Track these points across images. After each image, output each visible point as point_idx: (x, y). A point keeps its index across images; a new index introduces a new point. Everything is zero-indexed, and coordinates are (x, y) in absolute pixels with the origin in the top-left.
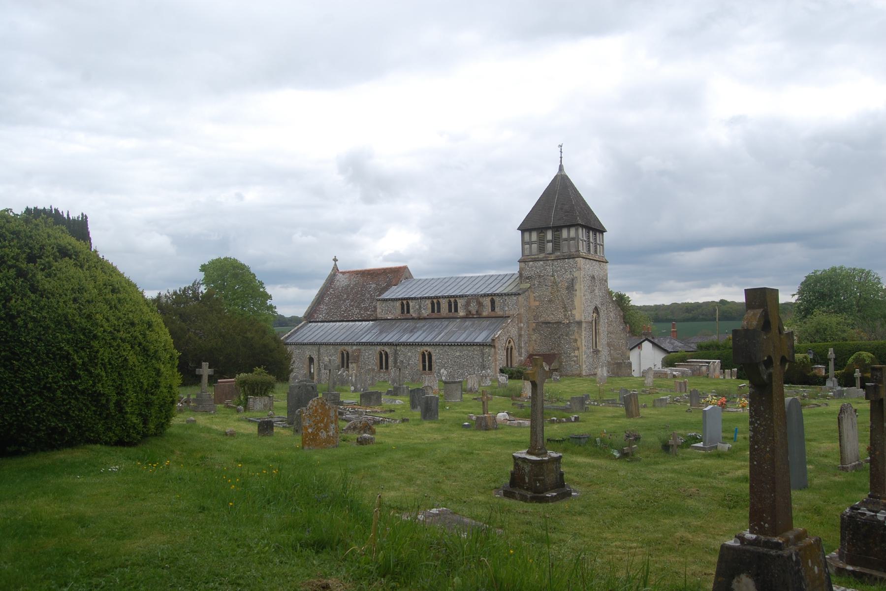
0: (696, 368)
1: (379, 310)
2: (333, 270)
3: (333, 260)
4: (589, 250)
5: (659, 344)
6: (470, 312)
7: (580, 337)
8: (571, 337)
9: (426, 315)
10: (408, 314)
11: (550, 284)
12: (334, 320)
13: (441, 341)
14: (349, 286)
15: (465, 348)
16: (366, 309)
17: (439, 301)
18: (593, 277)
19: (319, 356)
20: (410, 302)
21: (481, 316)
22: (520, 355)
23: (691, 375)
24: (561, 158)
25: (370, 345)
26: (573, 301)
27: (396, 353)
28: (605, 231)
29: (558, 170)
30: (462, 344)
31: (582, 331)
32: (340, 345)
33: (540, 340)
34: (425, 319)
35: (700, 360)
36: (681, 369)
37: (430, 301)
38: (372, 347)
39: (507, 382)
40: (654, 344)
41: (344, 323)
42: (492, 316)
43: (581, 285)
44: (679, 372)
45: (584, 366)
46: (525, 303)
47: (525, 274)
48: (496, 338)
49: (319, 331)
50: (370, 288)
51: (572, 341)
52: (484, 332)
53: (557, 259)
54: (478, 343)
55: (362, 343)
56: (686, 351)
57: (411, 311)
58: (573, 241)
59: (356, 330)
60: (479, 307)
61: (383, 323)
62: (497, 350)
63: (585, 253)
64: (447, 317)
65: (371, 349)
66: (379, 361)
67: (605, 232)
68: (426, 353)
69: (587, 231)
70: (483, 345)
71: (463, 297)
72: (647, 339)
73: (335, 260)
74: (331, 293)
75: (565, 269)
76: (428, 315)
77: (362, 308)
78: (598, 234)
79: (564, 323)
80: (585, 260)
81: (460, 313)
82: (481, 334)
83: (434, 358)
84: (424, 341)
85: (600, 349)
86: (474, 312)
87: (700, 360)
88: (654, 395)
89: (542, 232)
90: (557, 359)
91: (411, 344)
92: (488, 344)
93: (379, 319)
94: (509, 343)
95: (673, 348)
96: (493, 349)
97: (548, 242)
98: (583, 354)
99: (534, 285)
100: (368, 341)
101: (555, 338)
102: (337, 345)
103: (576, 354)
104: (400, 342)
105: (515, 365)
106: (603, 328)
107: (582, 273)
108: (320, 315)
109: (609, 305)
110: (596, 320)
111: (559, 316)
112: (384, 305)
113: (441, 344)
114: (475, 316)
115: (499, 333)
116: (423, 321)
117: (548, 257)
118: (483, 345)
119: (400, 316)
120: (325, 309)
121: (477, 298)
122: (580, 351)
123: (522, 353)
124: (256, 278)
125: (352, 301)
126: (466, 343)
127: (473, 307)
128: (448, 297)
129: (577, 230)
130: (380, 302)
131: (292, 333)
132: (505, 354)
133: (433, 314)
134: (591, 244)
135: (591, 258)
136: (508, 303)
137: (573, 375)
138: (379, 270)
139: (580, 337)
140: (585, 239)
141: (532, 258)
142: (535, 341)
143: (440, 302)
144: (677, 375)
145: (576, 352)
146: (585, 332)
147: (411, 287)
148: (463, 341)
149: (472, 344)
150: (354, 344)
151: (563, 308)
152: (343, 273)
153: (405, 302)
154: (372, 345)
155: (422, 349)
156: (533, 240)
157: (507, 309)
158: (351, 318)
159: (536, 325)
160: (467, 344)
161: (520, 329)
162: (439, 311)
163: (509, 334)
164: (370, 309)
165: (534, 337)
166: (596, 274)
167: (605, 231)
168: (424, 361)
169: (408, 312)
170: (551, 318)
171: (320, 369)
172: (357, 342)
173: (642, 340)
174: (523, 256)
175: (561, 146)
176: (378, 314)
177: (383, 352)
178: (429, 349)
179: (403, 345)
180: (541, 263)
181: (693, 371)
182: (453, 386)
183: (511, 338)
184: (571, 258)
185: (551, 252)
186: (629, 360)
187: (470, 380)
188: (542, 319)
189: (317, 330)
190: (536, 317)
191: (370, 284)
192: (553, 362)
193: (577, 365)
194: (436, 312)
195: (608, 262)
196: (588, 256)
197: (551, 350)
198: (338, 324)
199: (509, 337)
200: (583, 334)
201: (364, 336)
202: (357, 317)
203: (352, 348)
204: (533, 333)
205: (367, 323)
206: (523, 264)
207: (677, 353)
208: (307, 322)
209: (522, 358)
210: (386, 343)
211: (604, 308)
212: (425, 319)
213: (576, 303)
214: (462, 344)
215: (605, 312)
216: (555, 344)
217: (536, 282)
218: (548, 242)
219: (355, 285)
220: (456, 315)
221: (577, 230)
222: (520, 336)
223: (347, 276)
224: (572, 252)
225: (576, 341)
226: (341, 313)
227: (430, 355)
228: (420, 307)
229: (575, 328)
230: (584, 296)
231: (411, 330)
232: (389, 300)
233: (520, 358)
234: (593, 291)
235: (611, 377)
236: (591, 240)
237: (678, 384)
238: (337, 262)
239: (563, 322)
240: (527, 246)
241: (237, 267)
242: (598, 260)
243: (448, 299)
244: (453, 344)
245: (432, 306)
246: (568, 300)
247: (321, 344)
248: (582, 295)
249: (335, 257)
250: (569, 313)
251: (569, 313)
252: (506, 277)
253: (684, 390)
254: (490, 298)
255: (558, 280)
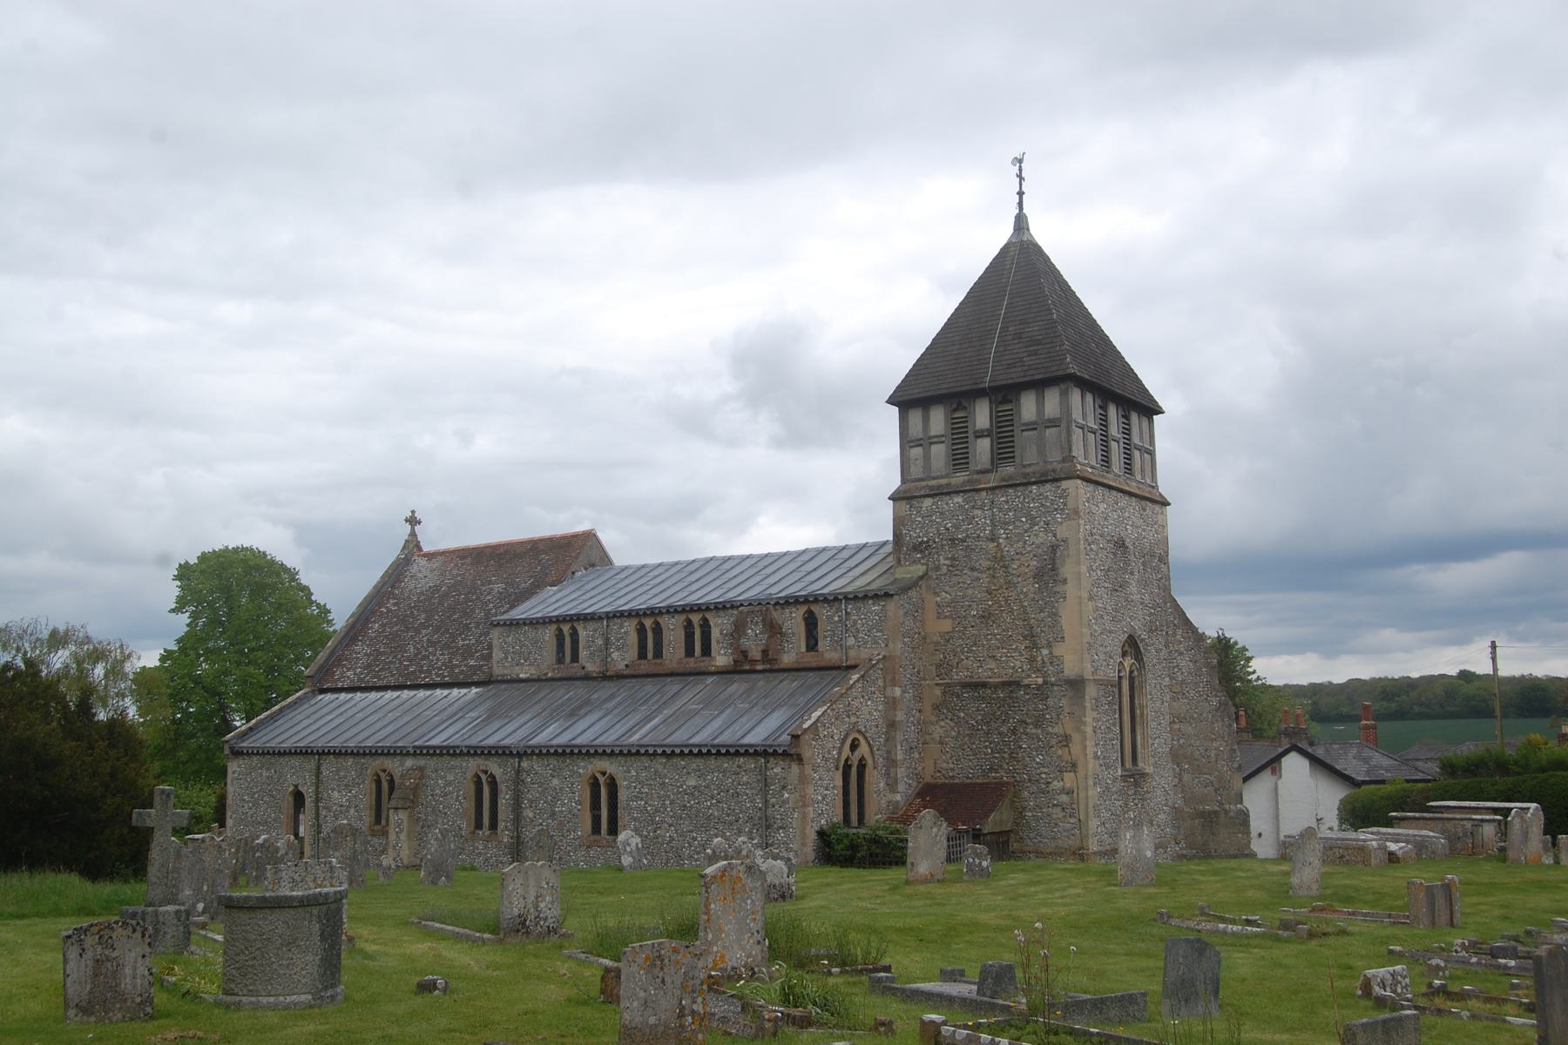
0: (1460, 830)
1: (497, 654)
2: (404, 547)
3: (407, 520)
4: (1106, 461)
5: (1328, 761)
6: (744, 653)
7: (1078, 730)
8: (1050, 729)
9: (621, 666)
10: (575, 664)
11: (986, 564)
12: (380, 683)
13: (646, 741)
14: (437, 589)
15: (712, 762)
16: (468, 652)
17: (657, 624)
18: (1120, 544)
19: (317, 787)
20: (580, 628)
21: (776, 667)
22: (892, 786)
23: (1448, 852)
24: (1021, 194)
25: (448, 754)
26: (1055, 615)
27: (518, 780)
28: (1159, 411)
29: (1011, 231)
30: (704, 750)
31: (1084, 707)
32: (371, 754)
33: (956, 738)
34: (619, 677)
35: (1473, 804)
36: (1411, 832)
37: (635, 622)
38: (454, 762)
39: (792, 880)
40: (1315, 761)
41: (406, 694)
42: (808, 665)
43: (1078, 563)
44: (1407, 842)
45: (1094, 823)
46: (909, 623)
47: (913, 535)
48: (806, 730)
49: (329, 718)
50: (489, 594)
51: (1053, 742)
52: (775, 715)
53: (1007, 485)
54: (751, 746)
55: (434, 747)
56: (1408, 781)
57: (583, 653)
58: (1054, 429)
59: (428, 713)
60: (769, 637)
61: (505, 690)
62: (808, 769)
63: (1092, 467)
64: (682, 670)
65: (453, 768)
66: (473, 804)
67: (1157, 414)
68: (602, 779)
69: (1098, 402)
70: (765, 754)
71: (724, 608)
72: (1294, 748)
73: (413, 521)
74: (389, 611)
75: (1028, 515)
76: (627, 666)
77: (459, 649)
78: (1134, 417)
79: (1028, 686)
80: (1091, 487)
81: (717, 658)
82: (766, 720)
83: (623, 795)
84: (595, 743)
85: (1149, 770)
86: (756, 654)
87: (1473, 804)
88: (1331, 941)
89: (959, 407)
90: (1007, 801)
91: (560, 751)
92: (780, 751)
93: (499, 682)
94: (854, 746)
95: (1368, 772)
96: (795, 768)
97: (980, 435)
98: (1091, 782)
99: (938, 568)
100: (445, 744)
101: (1000, 734)
102: (364, 754)
103: (1068, 785)
104: (529, 747)
105: (876, 815)
106: (1156, 703)
107: (1084, 527)
108: (349, 670)
109: (1175, 634)
110: (1132, 679)
111: (1014, 663)
112: (510, 638)
113: (642, 751)
114: (759, 667)
115: (818, 713)
116: (611, 684)
117: (979, 482)
118: (765, 754)
119: (553, 670)
120: (366, 654)
121: (766, 610)
122: (1081, 774)
123: (896, 780)
124: (313, 598)
125: (437, 629)
126: (713, 746)
127: (754, 639)
128: (684, 611)
129: (1064, 395)
130: (499, 629)
131: (262, 722)
132: (839, 782)
133: (643, 661)
134: (1114, 445)
135: (1113, 484)
136: (855, 622)
137: (1057, 854)
138: (521, 543)
139: (1078, 730)
140: (1091, 424)
141: (931, 488)
142: (941, 743)
143: (662, 624)
144: (1400, 853)
145: (1069, 778)
146: (1095, 714)
147: (593, 589)
148: (708, 740)
149: (732, 750)
150: (408, 754)
151: (1025, 638)
152: (431, 556)
153: (566, 628)
154: (454, 755)
155: (590, 767)
156: (933, 433)
157: (851, 641)
158: (425, 678)
159: (944, 693)
160: (718, 751)
161: (892, 704)
162: (658, 653)
163: (853, 719)
164: (476, 652)
165: (937, 731)
166: (1130, 534)
167: (1159, 411)
168: (595, 805)
169: (575, 658)
170: (988, 671)
171: (319, 826)
172: (413, 747)
173: (1280, 750)
174: (904, 481)
175: (1020, 161)
176: (495, 666)
177: (484, 777)
178: (610, 766)
179: (536, 755)
180: (956, 500)
181: (1453, 839)
182: (274, 923)
183: (859, 732)
184: (1047, 481)
185: (988, 466)
186: (1241, 803)
187: (519, 881)
188: (959, 676)
189: (327, 714)
190: (942, 668)
191: (490, 582)
192: (991, 811)
193: (1073, 820)
194: (650, 655)
195: (1169, 504)
196: (1103, 476)
197: (991, 770)
198: (389, 695)
199: (854, 728)
200: (1088, 719)
201: (444, 726)
202: (438, 675)
203: (402, 765)
204: (934, 719)
205: (464, 691)
206: (904, 506)
207: (1381, 786)
208: (313, 691)
209: (898, 797)
210: (493, 747)
211: (1159, 641)
212: (619, 677)
213: (1065, 622)
214: (704, 750)
215: (1163, 654)
216: (1001, 751)
217: (942, 561)
218: (980, 435)
219: (454, 585)
220: (704, 664)
221: (1064, 395)
222: (892, 725)
223: (436, 564)
224: (1052, 463)
225: (1065, 740)
226: (401, 663)
227: (612, 785)
228: (607, 642)
229: (1064, 702)
230: (1090, 599)
231: (573, 709)
232: (525, 624)
233: (890, 797)
234: (1119, 587)
235: (1185, 856)
236: (1114, 430)
237: (1422, 895)
238: (417, 528)
239: (1026, 682)
240: (916, 452)
241: (258, 568)
242: (1137, 492)
243: (683, 617)
244: (678, 751)
245: (639, 640)
246: (1042, 611)
247: (323, 753)
248: (1085, 595)
249: (413, 512)
250: (1045, 652)
251: (1045, 652)
252: (862, 552)
253: (1443, 917)
254: (803, 609)
255: (1009, 550)
